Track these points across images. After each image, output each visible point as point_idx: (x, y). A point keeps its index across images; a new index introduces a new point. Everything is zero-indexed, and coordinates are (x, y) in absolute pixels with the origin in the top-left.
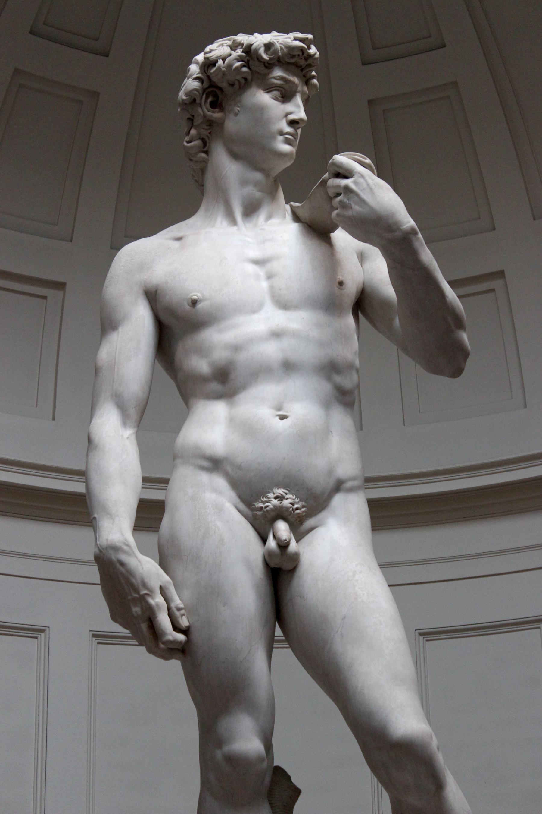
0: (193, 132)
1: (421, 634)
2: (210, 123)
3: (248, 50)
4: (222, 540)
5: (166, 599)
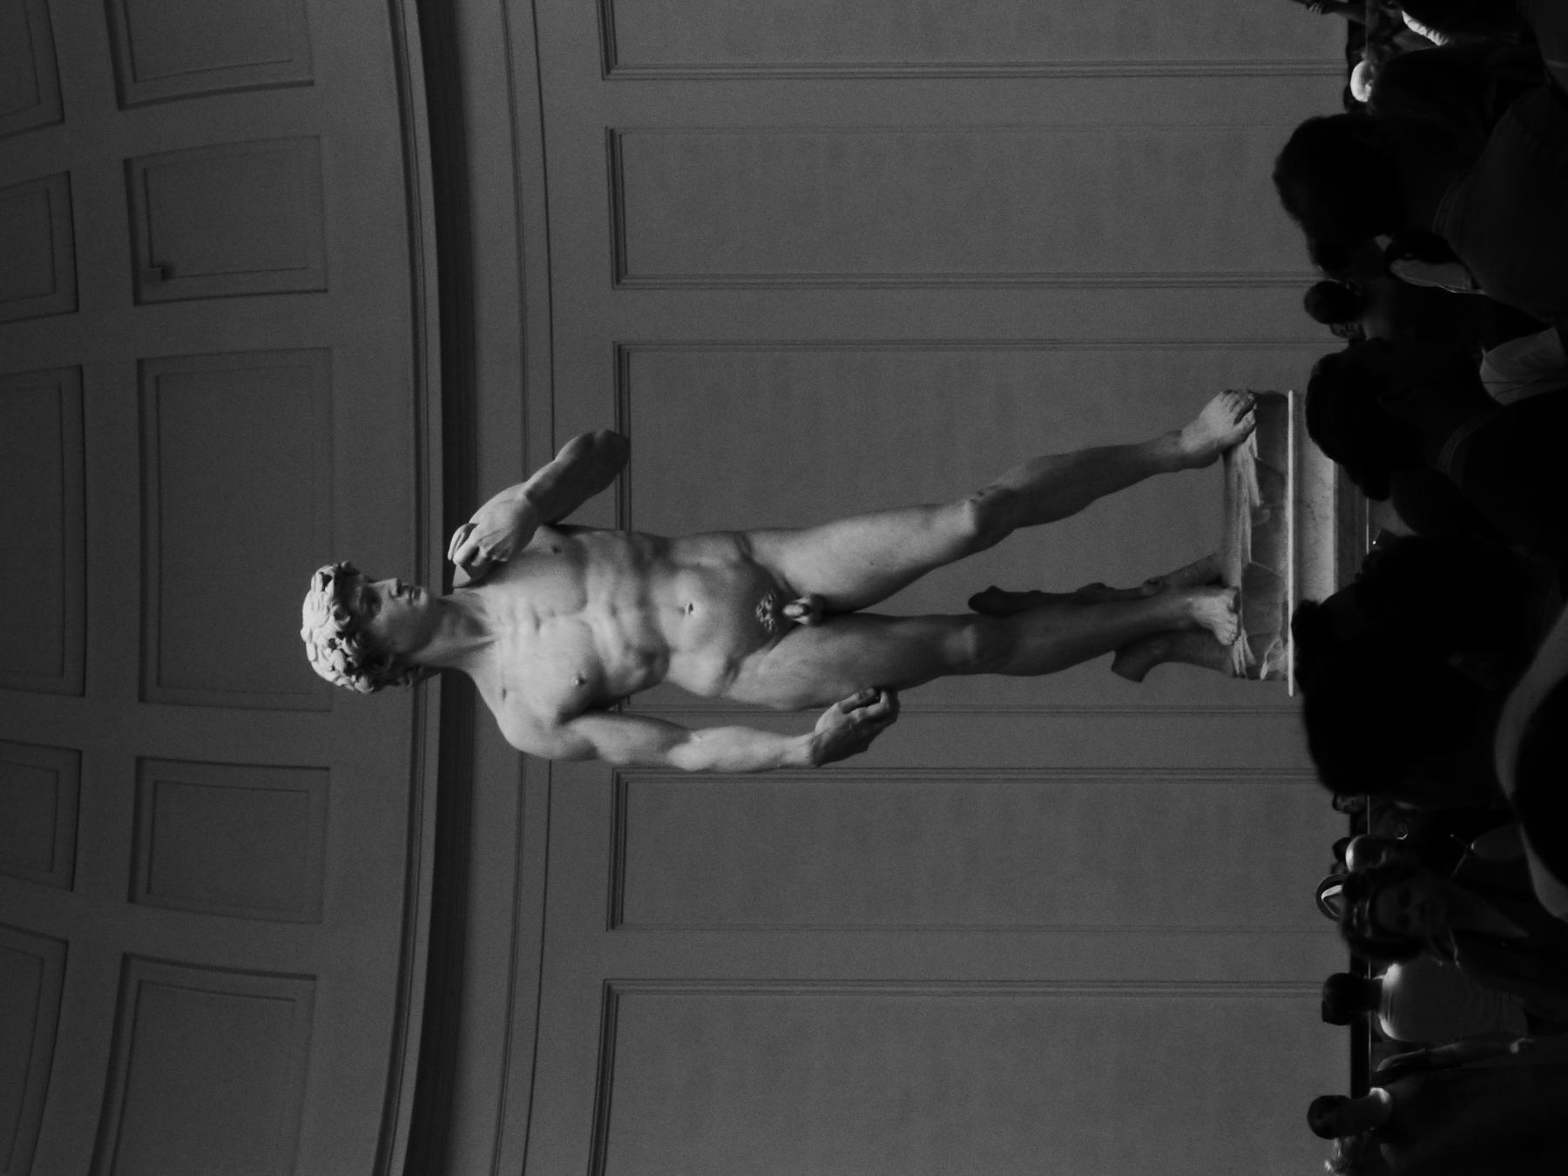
0: (401, 680)
1: (618, 281)
2: (395, 664)
3: (340, 635)
4: (804, 662)
5: (853, 707)
